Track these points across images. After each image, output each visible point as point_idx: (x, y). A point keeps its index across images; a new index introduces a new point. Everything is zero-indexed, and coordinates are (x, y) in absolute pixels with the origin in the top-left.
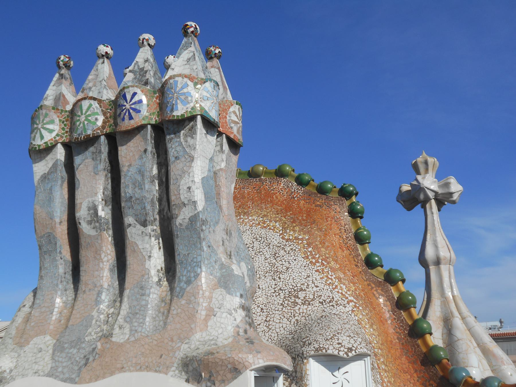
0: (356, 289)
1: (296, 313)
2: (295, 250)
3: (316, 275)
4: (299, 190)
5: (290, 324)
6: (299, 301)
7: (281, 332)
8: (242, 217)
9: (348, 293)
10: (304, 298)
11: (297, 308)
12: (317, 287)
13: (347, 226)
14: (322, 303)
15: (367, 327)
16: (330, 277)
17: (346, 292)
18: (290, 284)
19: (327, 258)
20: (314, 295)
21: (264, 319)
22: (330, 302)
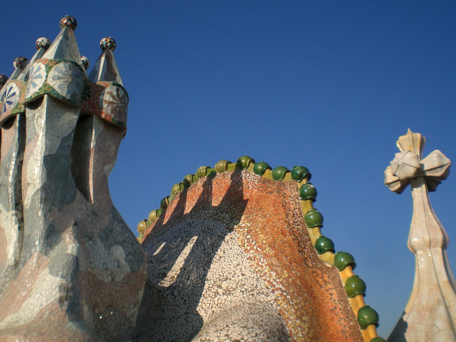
0: (289, 277)
1: (215, 304)
2: (234, 239)
3: (247, 263)
4: (255, 179)
5: (206, 316)
6: (221, 291)
7: (196, 325)
8: (200, 211)
9: (278, 280)
10: (227, 287)
11: (217, 298)
12: (243, 275)
13: (297, 210)
14: (243, 292)
15: (292, 318)
16: (260, 264)
17: (275, 280)
18: (217, 274)
19: (264, 244)
20: (237, 284)
21: (185, 311)
22: (252, 290)
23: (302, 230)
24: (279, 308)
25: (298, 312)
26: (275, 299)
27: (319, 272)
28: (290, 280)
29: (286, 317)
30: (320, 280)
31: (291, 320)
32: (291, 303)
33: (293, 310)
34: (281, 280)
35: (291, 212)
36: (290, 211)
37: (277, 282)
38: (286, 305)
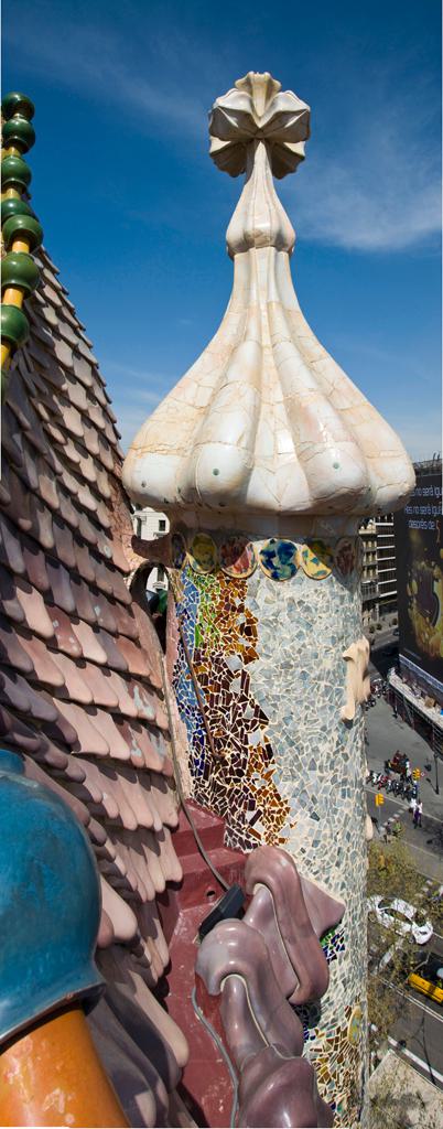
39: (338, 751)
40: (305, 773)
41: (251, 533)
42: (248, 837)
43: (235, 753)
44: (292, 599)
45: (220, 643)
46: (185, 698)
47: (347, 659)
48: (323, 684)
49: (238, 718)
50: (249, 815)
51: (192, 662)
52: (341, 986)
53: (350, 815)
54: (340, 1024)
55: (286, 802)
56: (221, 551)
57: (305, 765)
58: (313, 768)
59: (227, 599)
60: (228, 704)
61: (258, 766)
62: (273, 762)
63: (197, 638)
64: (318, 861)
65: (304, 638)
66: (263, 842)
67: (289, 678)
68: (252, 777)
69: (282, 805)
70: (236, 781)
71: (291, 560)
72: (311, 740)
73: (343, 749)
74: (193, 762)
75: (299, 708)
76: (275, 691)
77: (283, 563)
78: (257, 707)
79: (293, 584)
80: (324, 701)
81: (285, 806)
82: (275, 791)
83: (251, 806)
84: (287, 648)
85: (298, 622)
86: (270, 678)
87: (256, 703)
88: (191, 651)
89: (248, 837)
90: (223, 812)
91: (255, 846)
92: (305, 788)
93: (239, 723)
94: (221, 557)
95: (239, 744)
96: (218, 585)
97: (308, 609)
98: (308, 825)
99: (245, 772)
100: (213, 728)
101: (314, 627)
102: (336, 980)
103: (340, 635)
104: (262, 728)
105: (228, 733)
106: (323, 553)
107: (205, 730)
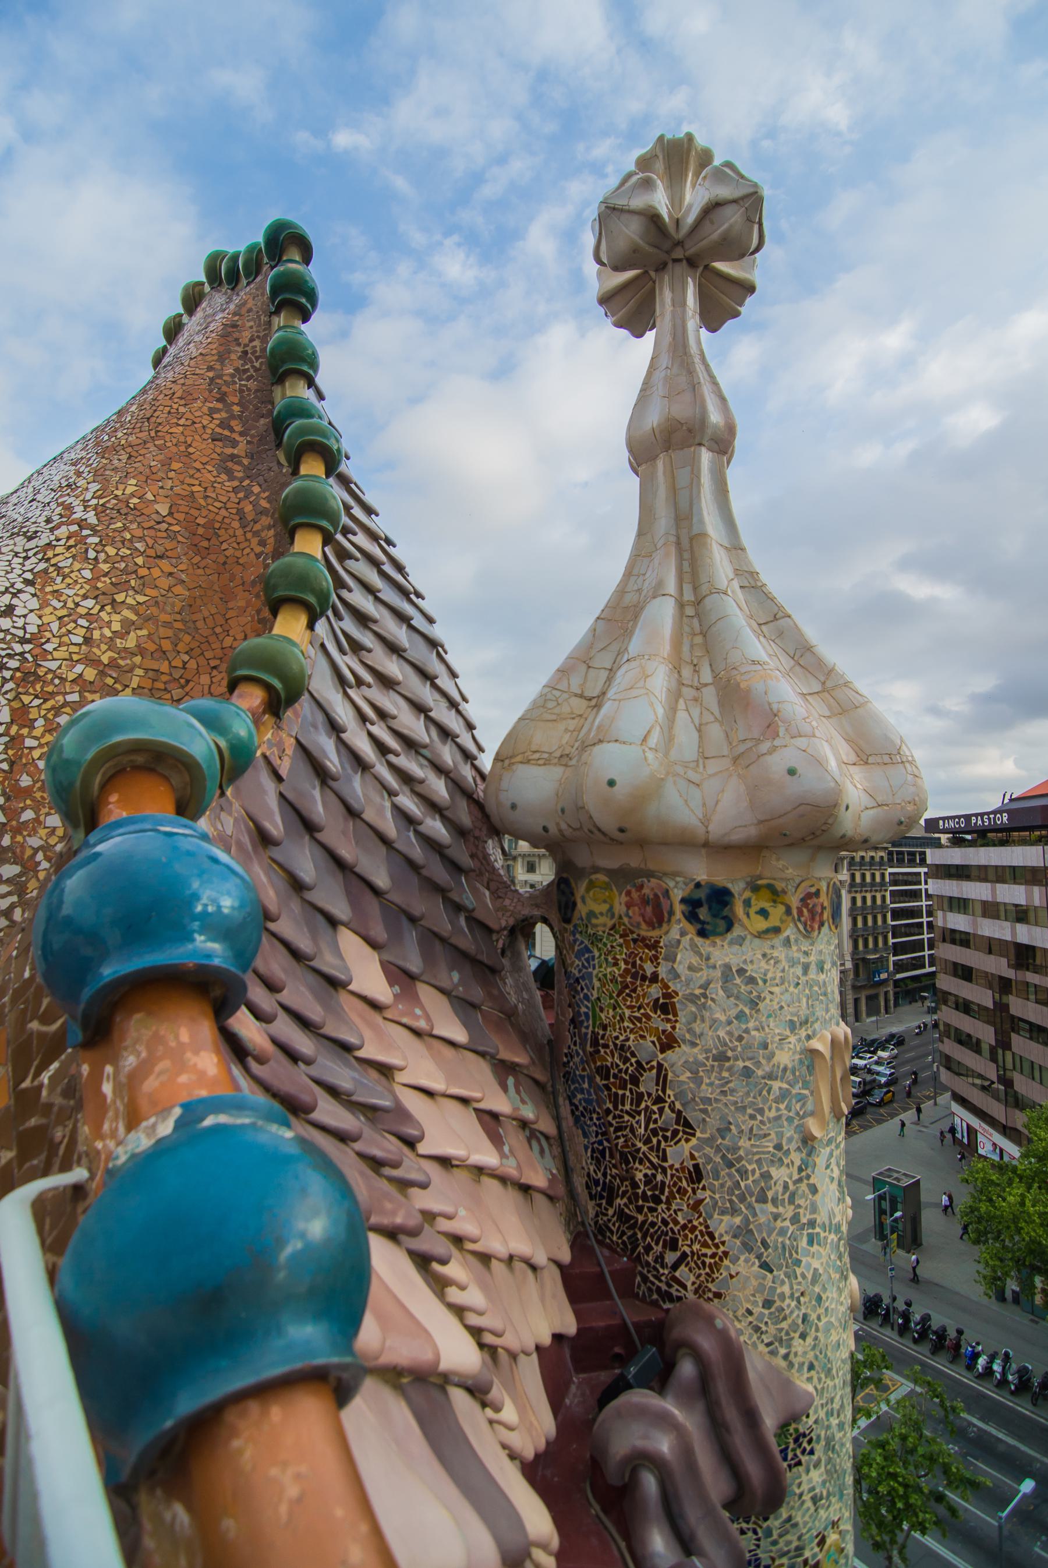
9: (94, 502)
13: (257, 343)
23: (257, 391)
24: (42, 566)
25: (103, 579)
26: (48, 544)
27: (256, 489)
28: (135, 500)
29: (48, 589)
30: (248, 508)
31: (62, 599)
32: (92, 554)
33: (87, 574)
34: (102, 501)
35: (240, 349)
36: (239, 345)
37: (85, 507)
38: (71, 560)
39: (800, 1180)
40: (750, 1207)
41: (665, 874)
42: (670, 1286)
43: (649, 1172)
44: (727, 967)
45: (626, 1024)
46: (579, 1096)
47: (814, 1052)
48: (776, 1085)
49: (652, 1126)
50: (671, 1257)
51: (589, 1049)
52: (809, 1504)
53: (821, 1271)
54: (807, 1554)
55: (723, 1243)
56: (624, 898)
57: (751, 1197)
58: (762, 1199)
59: (634, 964)
60: (638, 1105)
61: (682, 1192)
62: (704, 1188)
63: (594, 1016)
64: (772, 1329)
65: (748, 1022)
66: (691, 1296)
67: (725, 1074)
68: (674, 1207)
69: (717, 1246)
70: (652, 1210)
71: (726, 912)
72: (759, 1162)
73: (808, 1177)
74: (591, 1182)
75: (740, 1118)
76: (706, 1091)
77: (715, 916)
78: (679, 1112)
79: (731, 943)
80: (778, 1109)
81: (722, 1248)
82: (707, 1227)
83: (673, 1245)
84: (722, 1033)
85: (737, 998)
86: (697, 1072)
87: (678, 1106)
88: (586, 1034)
89: (670, 1286)
90: (633, 1250)
91: (679, 1299)
92: (751, 1226)
93: (655, 1132)
94: (624, 909)
95: (655, 1160)
96: (621, 946)
97: (752, 980)
98: (756, 1277)
99: (664, 1198)
100: (618, 1137)
101: (761, 1006)
102: (801, 1495)
103: (803, 1018)
104: (687, 1140)
105: (639, 1145)
106: (775, 901)
107: (608, 1140)
